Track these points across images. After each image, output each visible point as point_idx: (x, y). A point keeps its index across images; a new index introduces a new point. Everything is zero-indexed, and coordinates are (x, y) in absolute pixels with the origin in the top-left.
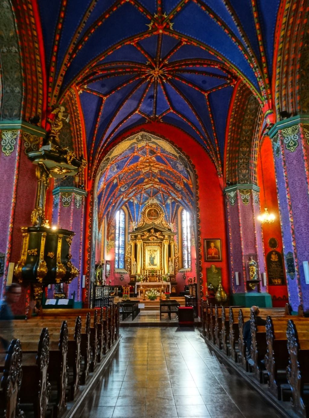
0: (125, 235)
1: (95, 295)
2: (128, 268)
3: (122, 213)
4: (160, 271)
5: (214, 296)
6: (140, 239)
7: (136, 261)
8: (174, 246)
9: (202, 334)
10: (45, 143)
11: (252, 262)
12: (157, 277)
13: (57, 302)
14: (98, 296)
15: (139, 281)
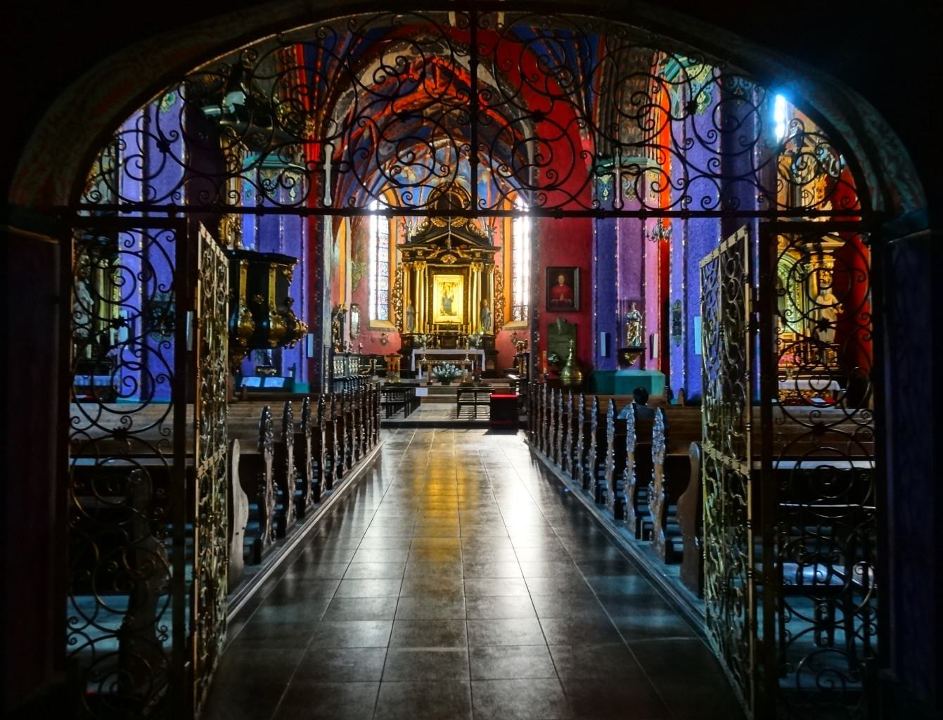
0: (389, 249)
1: (333, 372)
2: (398, 320)
5: (560, 375)
6: (421, 260)
8: (494, 274)
9: (527, 438)
10: (234, 87)
11: (635, 313)
13: (262, 382)
14: (338, 374)
15: (419, 346)
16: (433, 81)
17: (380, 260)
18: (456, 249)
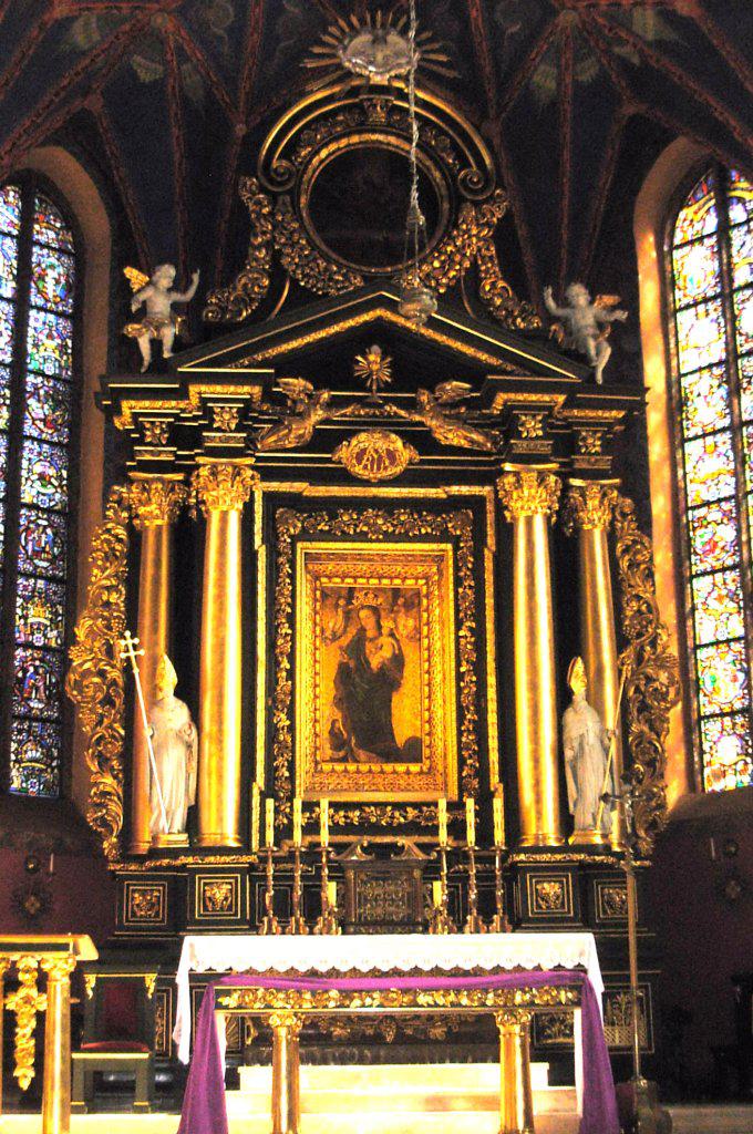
4: (470, 804)
7: (189, 691)
8: (612, 537)
12: (431, 871)
17: (28, 495)
18: (411, 405)
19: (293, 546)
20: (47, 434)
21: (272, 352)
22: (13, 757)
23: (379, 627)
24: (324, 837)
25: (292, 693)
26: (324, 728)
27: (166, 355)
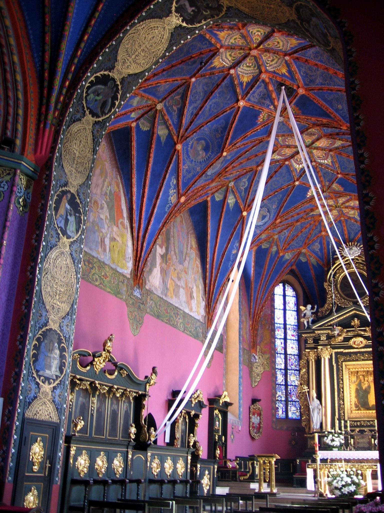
3: (290, 292)
7: (319, 397)
16: (272, 107)
17: (288, 353)
19: (342, 363)
20: (293, 338)
21: (331, 323)
22: (289, 410)
23: (364, 379)
24: (349, 429)
25: (343, 396)
26: (353, 403)
27: (310, 324)
